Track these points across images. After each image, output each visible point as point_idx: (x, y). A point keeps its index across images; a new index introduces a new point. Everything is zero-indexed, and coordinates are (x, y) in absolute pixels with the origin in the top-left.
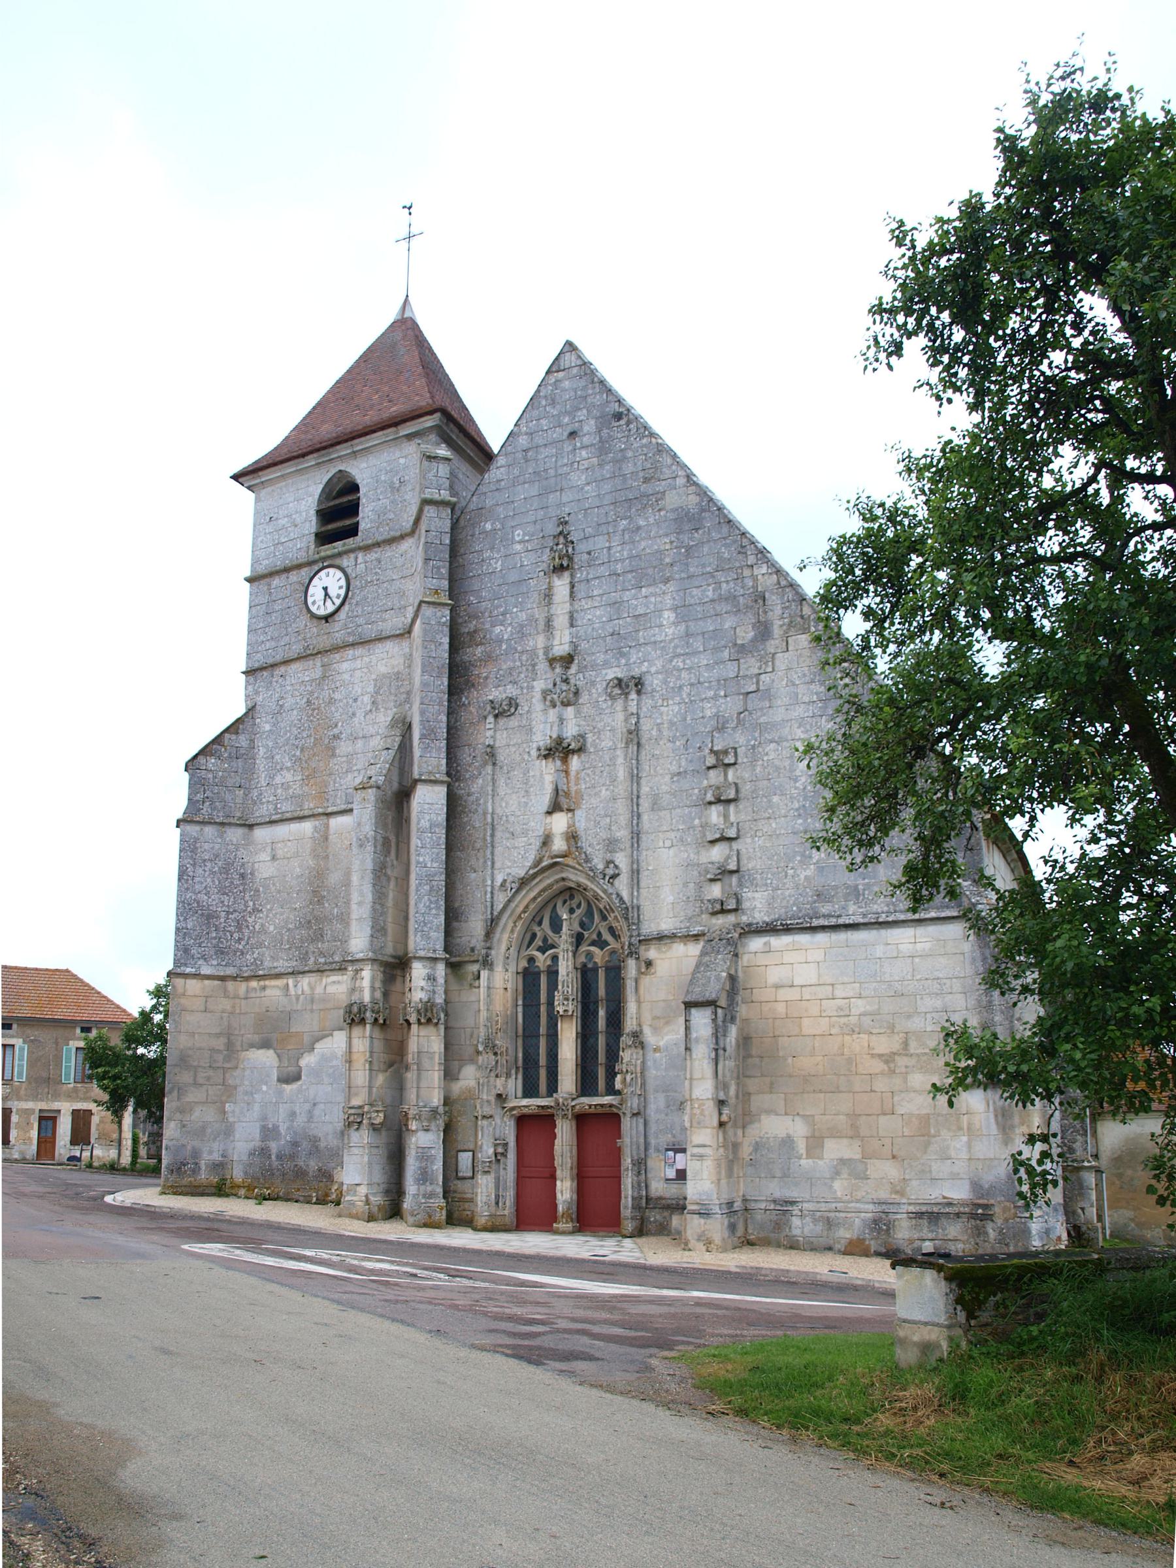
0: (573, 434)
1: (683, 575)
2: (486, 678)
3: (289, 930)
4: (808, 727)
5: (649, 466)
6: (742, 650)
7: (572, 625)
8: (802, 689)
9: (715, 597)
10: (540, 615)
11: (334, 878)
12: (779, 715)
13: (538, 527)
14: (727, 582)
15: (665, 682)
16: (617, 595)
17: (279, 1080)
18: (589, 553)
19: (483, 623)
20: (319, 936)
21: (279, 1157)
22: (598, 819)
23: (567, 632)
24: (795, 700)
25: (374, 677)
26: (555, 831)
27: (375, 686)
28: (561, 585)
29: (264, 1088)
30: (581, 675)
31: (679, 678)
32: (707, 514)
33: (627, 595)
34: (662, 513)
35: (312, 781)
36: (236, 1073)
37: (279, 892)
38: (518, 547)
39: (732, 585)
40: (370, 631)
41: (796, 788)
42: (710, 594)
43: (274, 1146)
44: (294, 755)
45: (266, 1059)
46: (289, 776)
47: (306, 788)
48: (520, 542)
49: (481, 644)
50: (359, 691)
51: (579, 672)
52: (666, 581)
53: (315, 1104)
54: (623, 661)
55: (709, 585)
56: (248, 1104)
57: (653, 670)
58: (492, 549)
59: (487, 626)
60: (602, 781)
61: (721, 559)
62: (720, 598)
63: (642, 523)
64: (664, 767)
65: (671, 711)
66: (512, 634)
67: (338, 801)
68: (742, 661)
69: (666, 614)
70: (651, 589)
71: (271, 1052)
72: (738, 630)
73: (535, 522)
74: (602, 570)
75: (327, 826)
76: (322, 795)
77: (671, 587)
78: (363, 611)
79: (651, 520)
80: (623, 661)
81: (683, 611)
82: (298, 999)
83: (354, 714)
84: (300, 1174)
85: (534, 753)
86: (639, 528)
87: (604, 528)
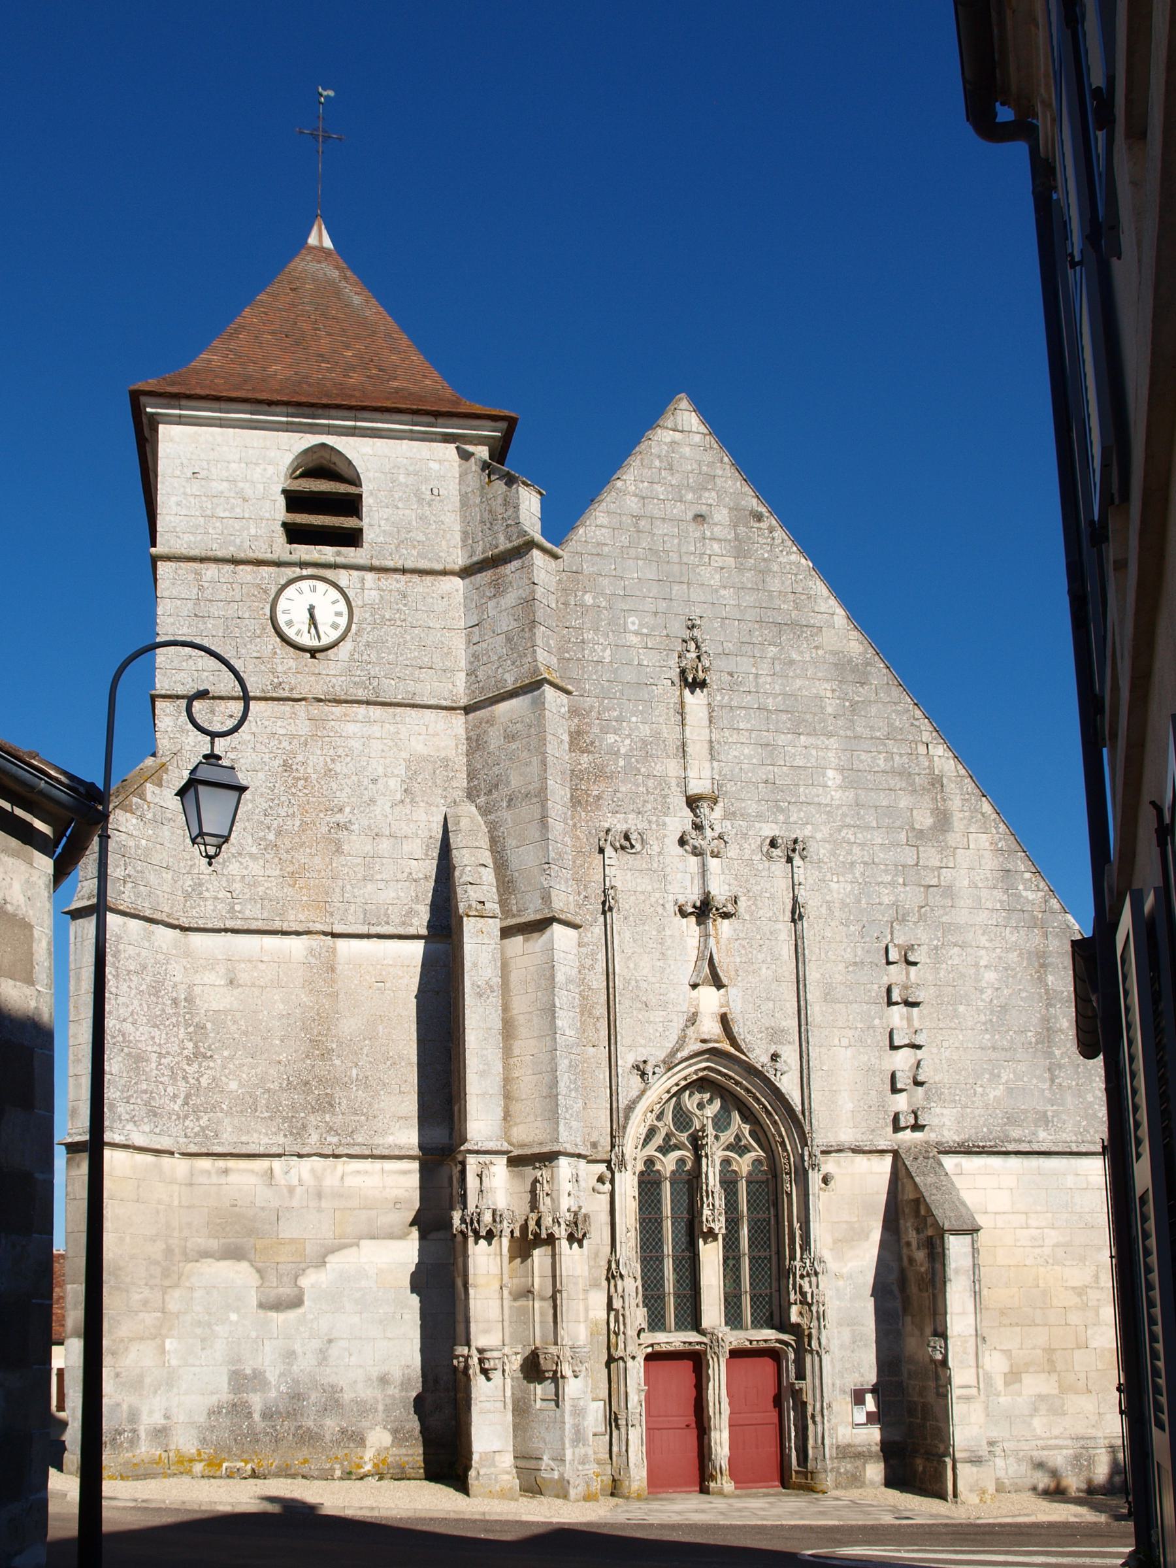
0: (700, 518)
1: (849, 733)
2: (599, 798)
3: (268, 1091)
4: (992, 935)
5: (800, 590)
6: (919, 836)
7: (712, 758)
8: (984, 893)
9: (888, 768)
10: (671, 735)
11: (349, 1026)
12: (961, 916)
13: (660, 620)
14: (901, 755)
15: (833, 853)
16: (770, 736)
17: (261, 1306)
18: (731, 674)
19: (589, 725)
20: (326, 1105)
21: (267, 1415)
22: (758, 1002)
23: (707, 765)
24: (978, 905)
25: (404, 755)
26: (702, 1009)
27: (408, 768)
28: (696, 701)
29: (234, 1317)
30: (728, 823)
31: (849, 853)
32: (873, 670)
33: (782, 739)
34: (820, 652)
35: (301, 882)
36: (177, 1293)
37: (246, 1033)
38: (634, 640)
39: (905, 759)
40: (392, 690)
41: (982, 1000)
42: (881, 762)
43: (256, 1402)
44: (264, 839)
45: (240, 1274)
46: (256, 868)
47: (289, 891)
48: (637, 633)
49: (589, 752)
50: (380, 771)
51: (725, 818)
52: (830, 735)
53: (330, 1341)
54: (781, 818)
55: (880, 753)
56: (203, 1340)
57: (819, 836)
58: (596, 630)
59: (596, 730)
60: (761, 957)
61: (890, 725)
62: (893, 771)
63: (795, 656)
64: (834, 953)
65: (840, 888)
66: (631, 750)
67: (351, 918)
68: (921, 848)
69: (830, 773)
70: (812, 740)
71: (244, 1265)
72: (915, 812)
73: (656, 613)
74: (748, 699)
75: (334, 951)
76: (323, 904)
77: (833, 743)
78: (380, 658)
79: (807, 657)
80: (781, 818)
81: (852, 776)
82: (291, 1190)
83: (372, 801)
84: (308, 1438)
85: (671, 908)
86: (792, 662)
87: (747, 648)
